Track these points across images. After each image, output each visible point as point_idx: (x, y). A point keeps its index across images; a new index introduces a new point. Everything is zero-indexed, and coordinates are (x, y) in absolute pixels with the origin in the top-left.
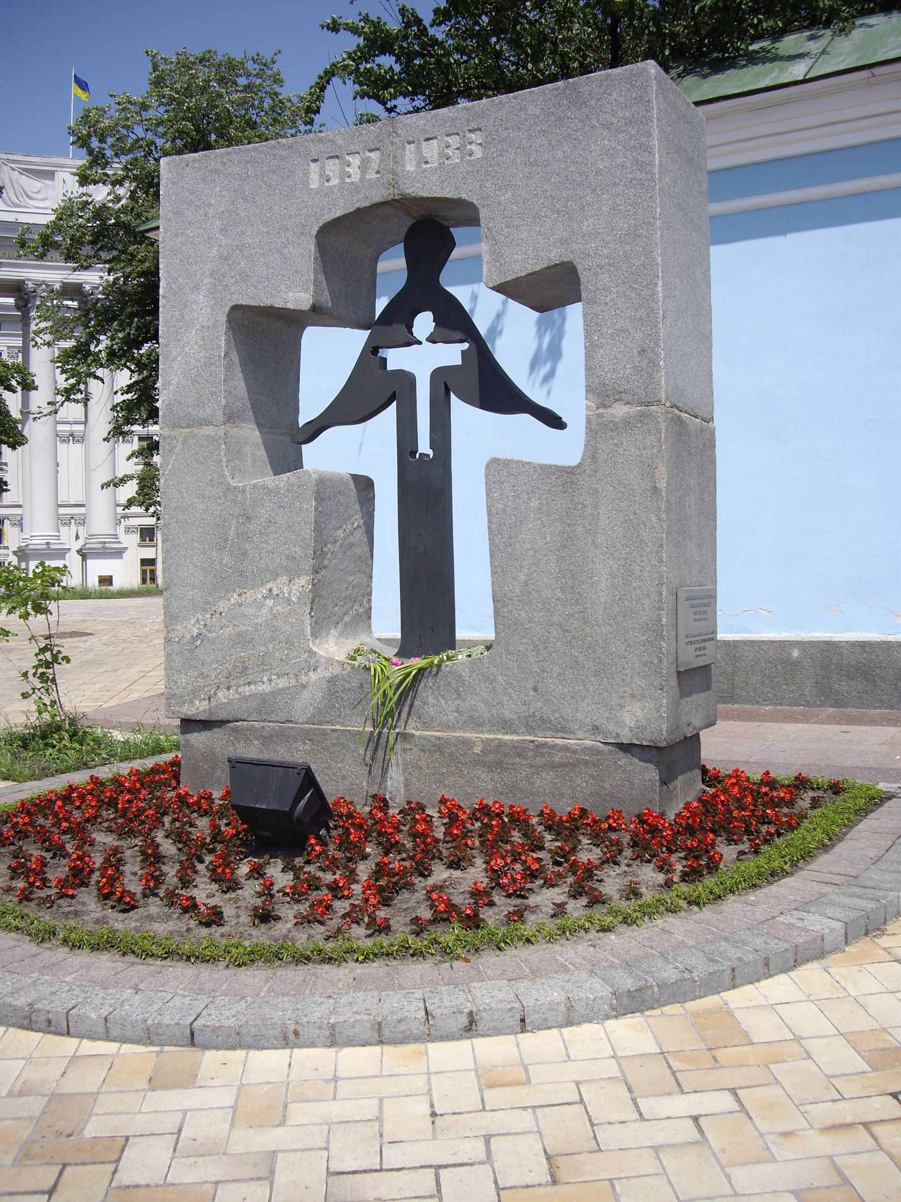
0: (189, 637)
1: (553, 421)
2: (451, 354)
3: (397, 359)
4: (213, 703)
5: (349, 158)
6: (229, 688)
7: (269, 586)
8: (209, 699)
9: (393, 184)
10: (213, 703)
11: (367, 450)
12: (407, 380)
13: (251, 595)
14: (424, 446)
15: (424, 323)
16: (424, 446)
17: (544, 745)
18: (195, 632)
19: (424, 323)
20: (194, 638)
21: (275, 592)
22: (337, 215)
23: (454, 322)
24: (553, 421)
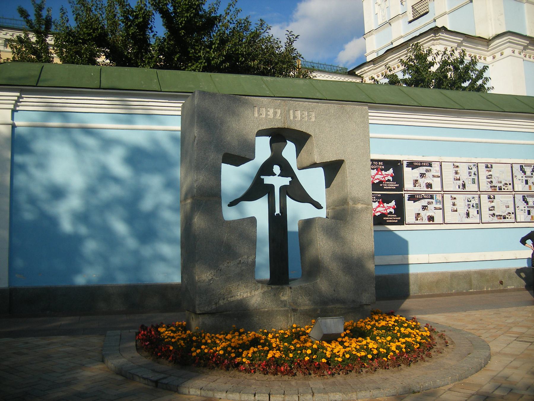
0: (207, 280)
1: (318, 206)
2: (286, 181)
3: (268, 180)
4: (218, 305)
5: (268, 109)
6: (224, 299)
7: (240, 259)
8: (216, 304)
9: (284, 123)
10: (218, 305)
11: (258, 210)
12: (272, 187)
13: (232, 264)
14: (278, 211)
15: (277, 169)
16: (278, 211)
17: (339, 308)
18: (210, 278)
19: (277, 169)
20: (210, 280)
21: (242, 262)
22: (265, 128)
23: (287, 170)
24: (318, 206)
